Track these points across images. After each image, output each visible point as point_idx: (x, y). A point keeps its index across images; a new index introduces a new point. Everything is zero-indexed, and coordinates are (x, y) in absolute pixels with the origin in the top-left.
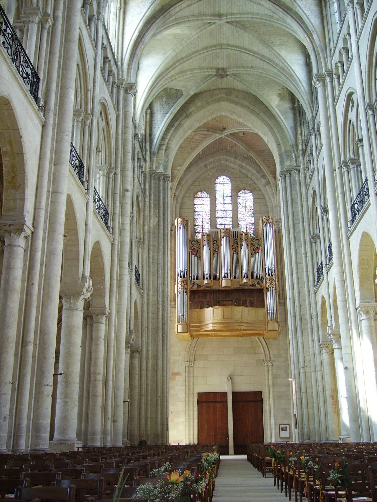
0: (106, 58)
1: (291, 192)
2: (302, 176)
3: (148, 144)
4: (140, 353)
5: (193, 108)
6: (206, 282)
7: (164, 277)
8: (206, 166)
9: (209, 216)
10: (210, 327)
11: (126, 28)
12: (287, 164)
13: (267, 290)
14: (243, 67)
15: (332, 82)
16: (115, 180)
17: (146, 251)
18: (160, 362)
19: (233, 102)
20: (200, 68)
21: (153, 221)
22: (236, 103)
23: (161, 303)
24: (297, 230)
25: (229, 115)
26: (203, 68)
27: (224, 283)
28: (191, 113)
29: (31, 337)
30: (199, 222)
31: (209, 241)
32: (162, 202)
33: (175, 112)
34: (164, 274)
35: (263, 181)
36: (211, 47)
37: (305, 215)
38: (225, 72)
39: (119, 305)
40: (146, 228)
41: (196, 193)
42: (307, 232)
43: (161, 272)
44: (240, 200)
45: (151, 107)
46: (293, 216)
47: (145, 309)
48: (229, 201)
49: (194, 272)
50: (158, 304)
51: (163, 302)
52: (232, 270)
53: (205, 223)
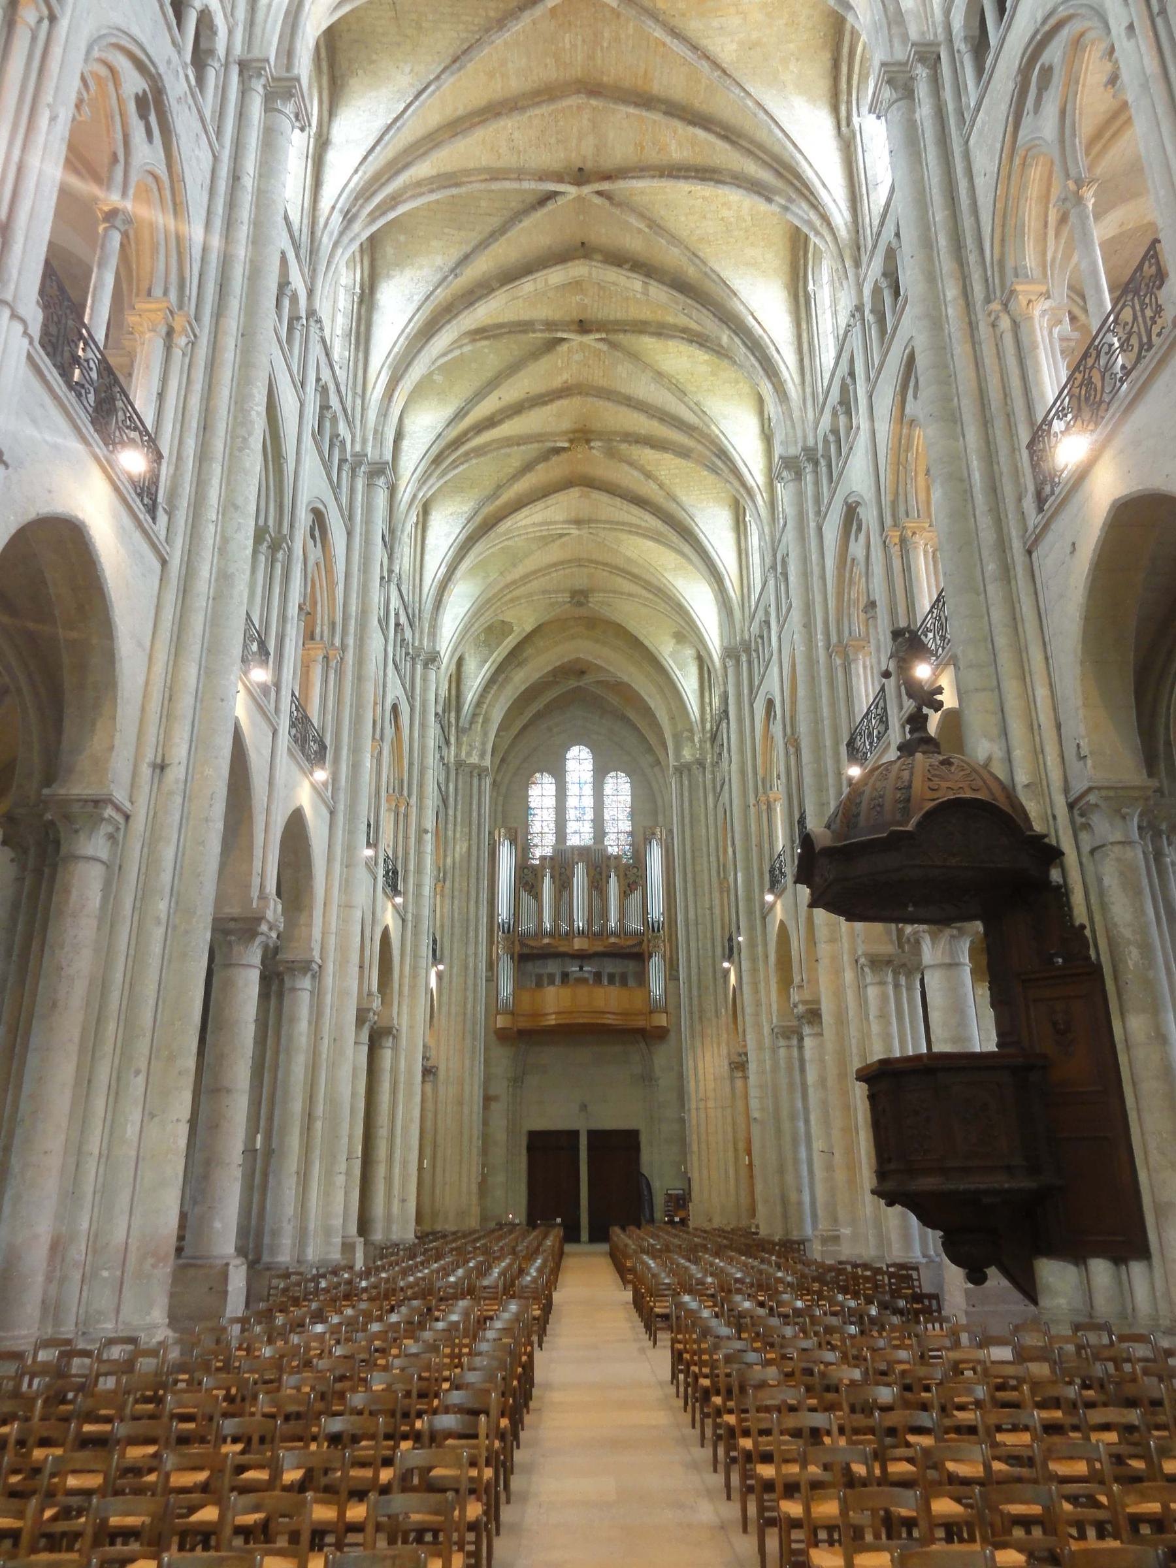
0: (397, 625)
1: (691, 802)
2: (709, 776)
3: (453, 714)
4: (435, 1074)
5: (530, 651)
6: (546, 941)
7: (476, 943)
8: (550, 729)
9: (553, 816)
10: (552, 1021)
11: (427, 557)
12: (687, 754)
13: (650, 957)
14: (615, 592)
15: (750, 663)
16: (406, 816)
17: (447, 901)
18: (467, 1088)
19: (597, 641)
20: (544, 592)
21: (461, 848)
23: (471, 987)
24: (698, 868)
25: (590, 658)
26: (549, 592)
27: (578, 944)
28: (526, 660)
29: (320, 1110)
30: (535, 828)
31: (552, 868)
32: (475, 814)
33: (500, 659)
34: (477, 937)
35: (650, 759)
36: (562, 563)
37: (712, 843)
38: (586, 597)
39: (412, 1016)
40: (449, 860)
41: (532, 775)
42: (714, 873)
43: (472, 934)
44: (608, 789)
45: (460, 662)
46: (693, 844)
47: (445, 998)
48: (588, 790)
50: (465, 989)
51: (475, 985)
52: (590, 921)
53: (546, 830)
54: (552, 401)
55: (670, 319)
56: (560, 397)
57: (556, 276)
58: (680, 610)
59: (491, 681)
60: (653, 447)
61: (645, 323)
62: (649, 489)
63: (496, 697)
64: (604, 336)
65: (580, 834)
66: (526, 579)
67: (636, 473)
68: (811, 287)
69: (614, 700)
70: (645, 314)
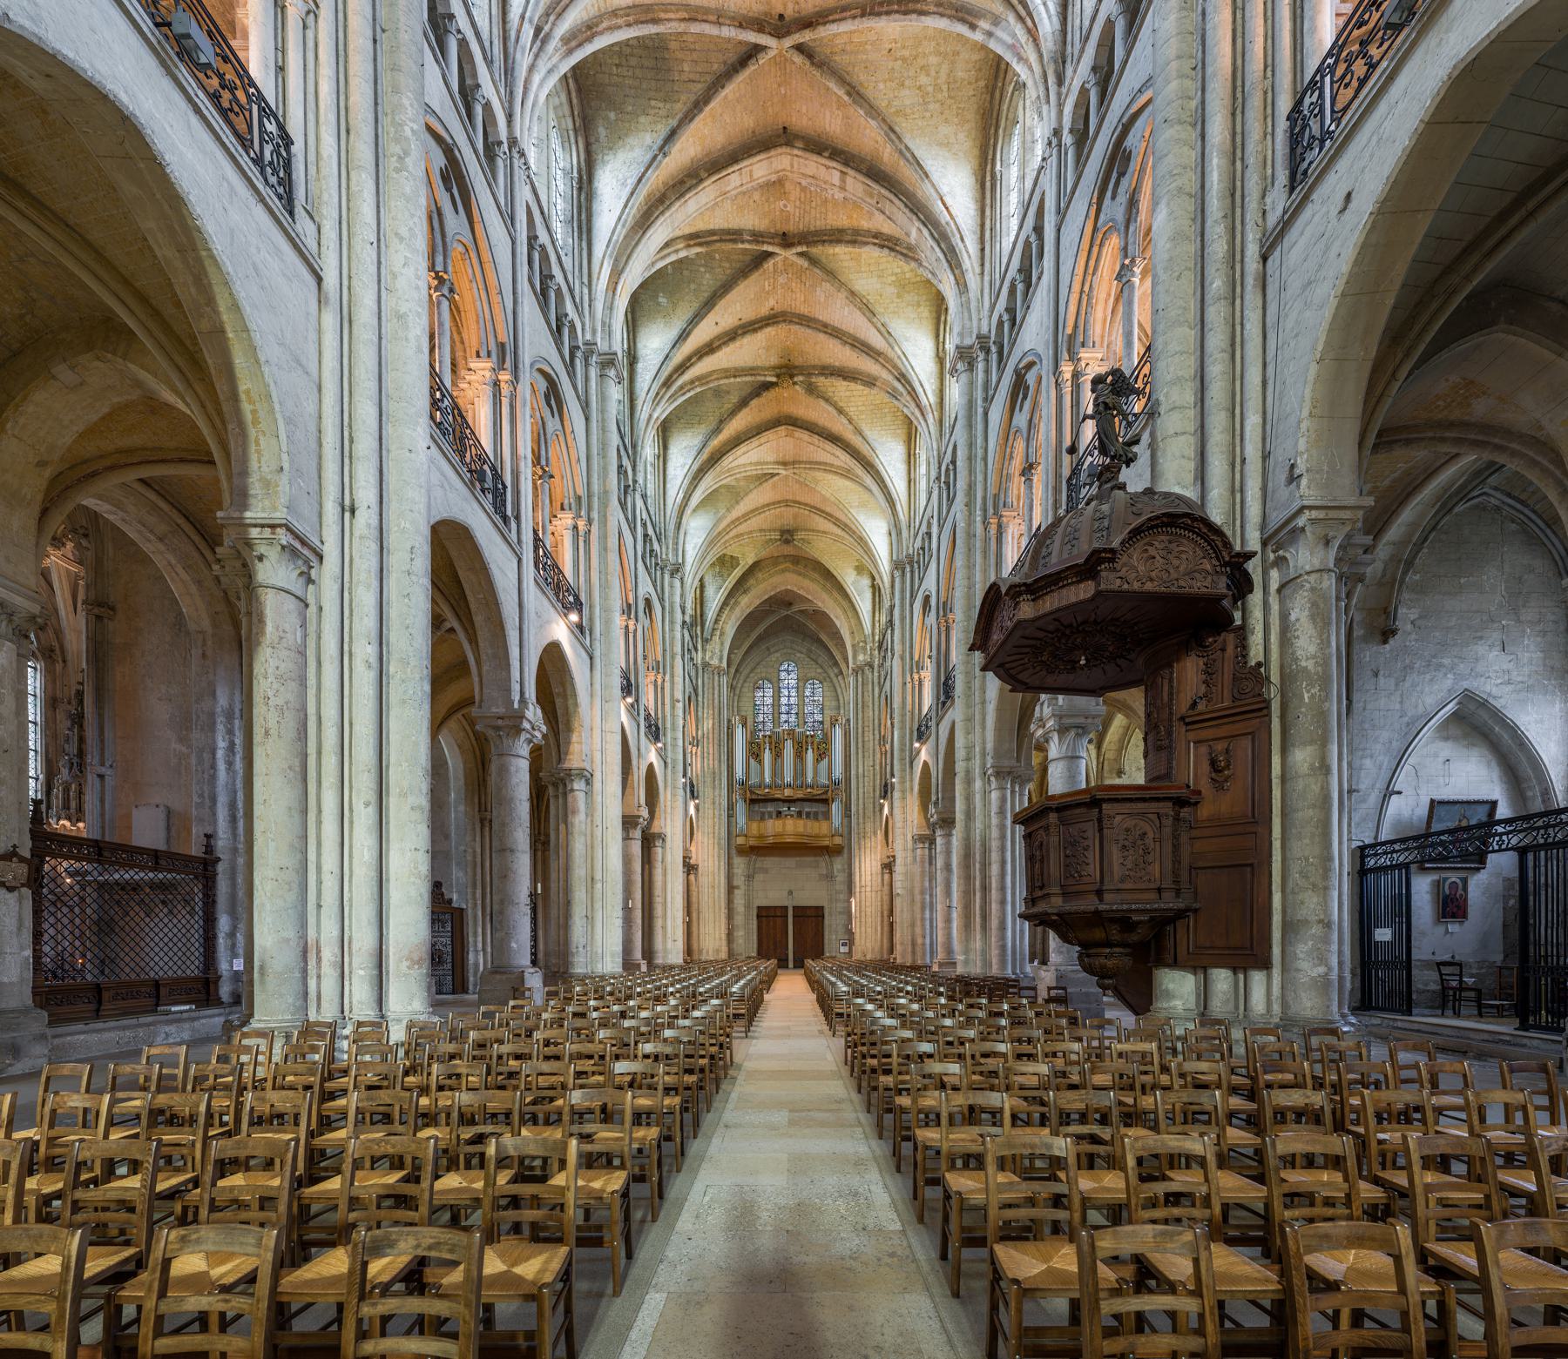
5: (752, 581)
22: (805, 576)
49: (754, 780)
54: (761, 328)
55: (865, 224)
56: (767, 325)
57: (760, 168)
58: (862, 542)
59: (725, 604)
60: (845, 378)
61: (841, 231)
62: (839, 426)
63: (729, 617)
64: (805, 249)
65: (789, 721)
66: (746, 517)
67: (830, 409)
68: (998, 167)
69: (812, 626)
70: (840, 219)
